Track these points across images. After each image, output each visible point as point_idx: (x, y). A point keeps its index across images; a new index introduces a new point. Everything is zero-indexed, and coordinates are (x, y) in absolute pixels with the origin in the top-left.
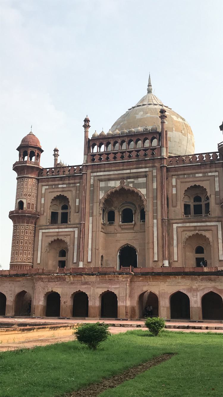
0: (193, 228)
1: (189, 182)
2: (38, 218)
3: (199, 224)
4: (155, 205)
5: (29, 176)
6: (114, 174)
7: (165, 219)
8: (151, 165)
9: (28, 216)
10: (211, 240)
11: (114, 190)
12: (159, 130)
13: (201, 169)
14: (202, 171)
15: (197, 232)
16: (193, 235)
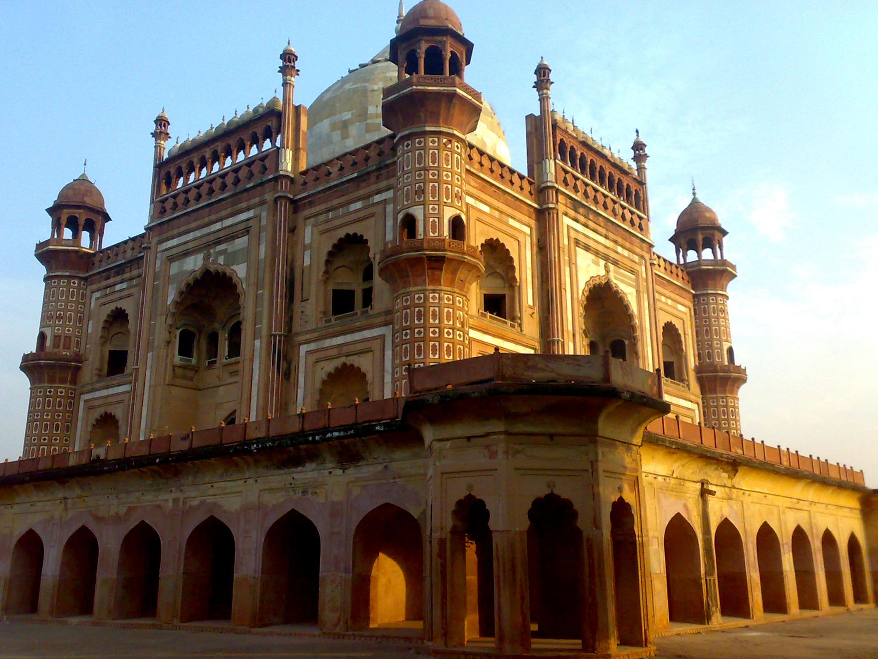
0: (335, 352)
1: (335, 228)
2: (78, 369)
3: (349, 338)
4: (258, 298)
5: (59, 274)
6: (195, 239)
7: (275, 336)
8: (257, 200)
9: (46, 365)
10: (369, 376)
11: (191, 280)
12: (280, 108)
13: (358, 188)
14: (361, 192)
15: (343, 359)
16: (337, 369)
